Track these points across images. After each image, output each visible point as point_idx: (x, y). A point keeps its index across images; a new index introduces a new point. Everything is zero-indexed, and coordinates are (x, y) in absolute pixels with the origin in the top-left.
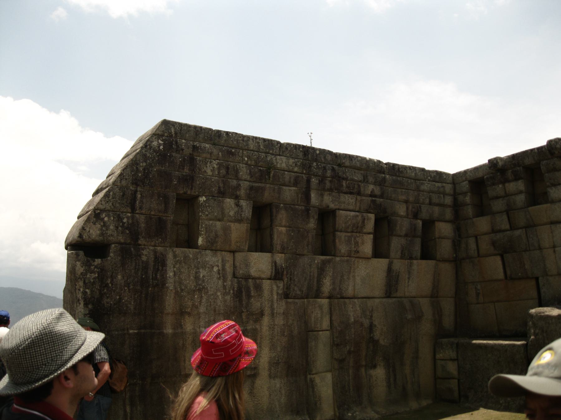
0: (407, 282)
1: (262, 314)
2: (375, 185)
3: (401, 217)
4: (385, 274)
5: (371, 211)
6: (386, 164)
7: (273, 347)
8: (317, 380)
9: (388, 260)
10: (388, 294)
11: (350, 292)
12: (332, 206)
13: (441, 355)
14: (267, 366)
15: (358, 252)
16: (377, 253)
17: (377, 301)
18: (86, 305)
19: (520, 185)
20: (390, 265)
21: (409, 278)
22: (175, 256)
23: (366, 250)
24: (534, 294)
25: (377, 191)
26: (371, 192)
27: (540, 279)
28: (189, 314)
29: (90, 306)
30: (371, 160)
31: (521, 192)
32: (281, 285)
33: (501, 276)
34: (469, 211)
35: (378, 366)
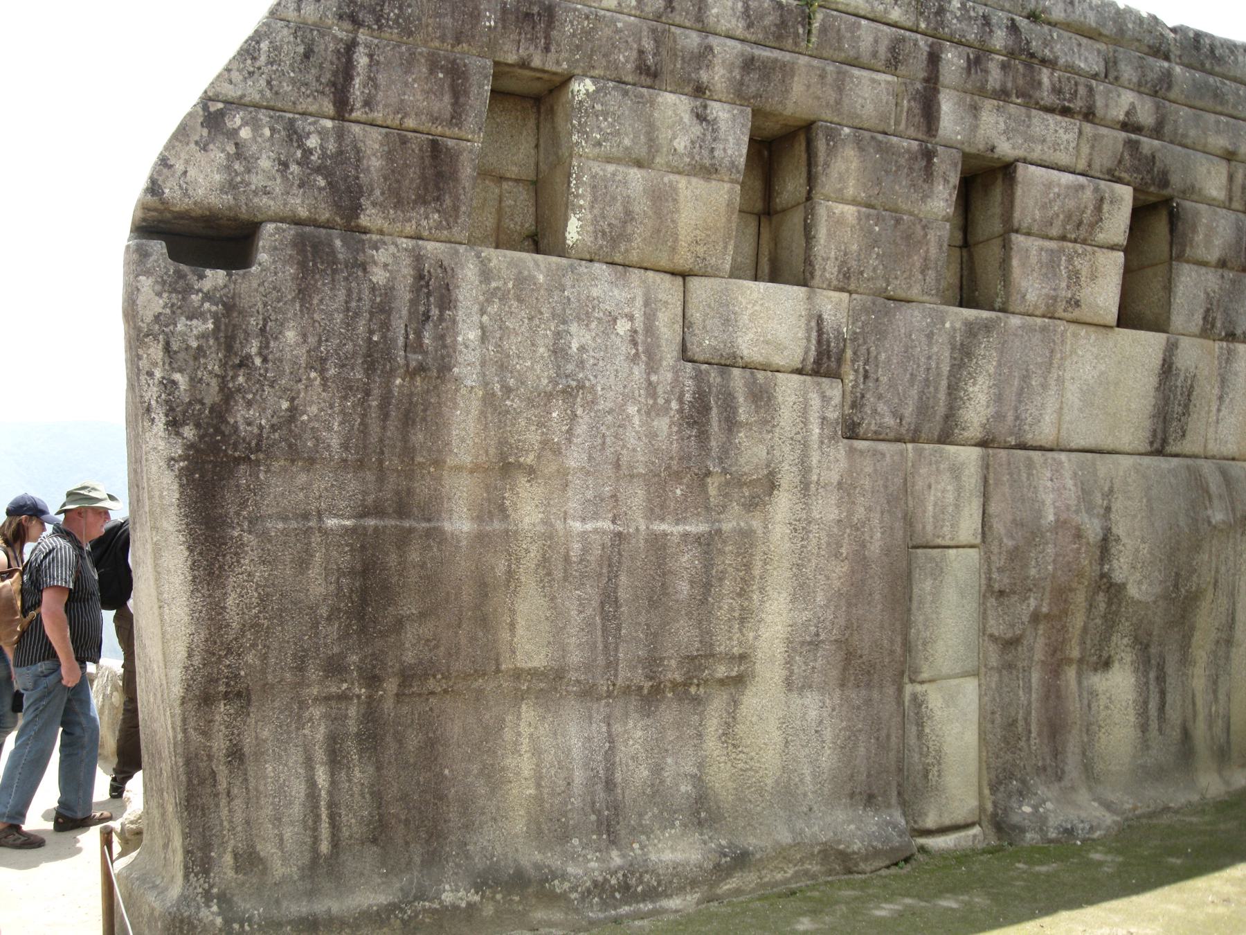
0: (1214, 409)
1: (771, 484)
2: (1139, 92)
3: (1211, 202)
4: (1153, 381)
5: (1123, 175)
6: (1174, 30)
7: (801, 592)
8: (934, 698)
9: (1164, 336)
10: (1159, 448)
11: (1045, 432)
12: (1006, 149)
14: (779, 649)
15: (1077, 304)
16: (1130, 316)
17: (1126, 462)
18: (174, 425)
20: (1171, 348)
21: (1221, 398)
22: (486, 275)
23: (1100, 301)
25: (1146, 114)
26: (1127, 114)
28: (531, 471)
29: (189, 432)
30: (1129, 11)
32: (834, 390)
35: (1116, 665)
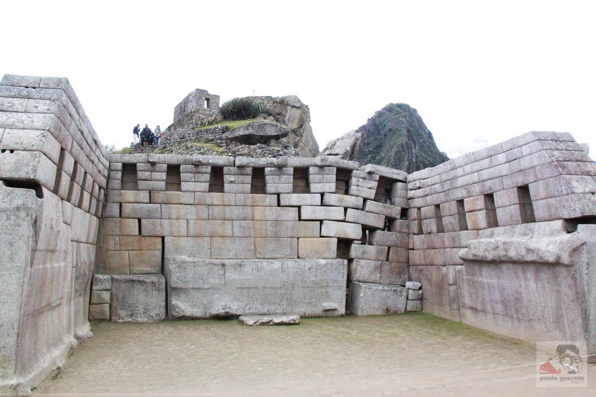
13: (98, 287)
19: (164, 176)
24: (161, 247)
27: (166, 238)
31: (163, 180)
33: (137, 233)
34: (116, 183)
